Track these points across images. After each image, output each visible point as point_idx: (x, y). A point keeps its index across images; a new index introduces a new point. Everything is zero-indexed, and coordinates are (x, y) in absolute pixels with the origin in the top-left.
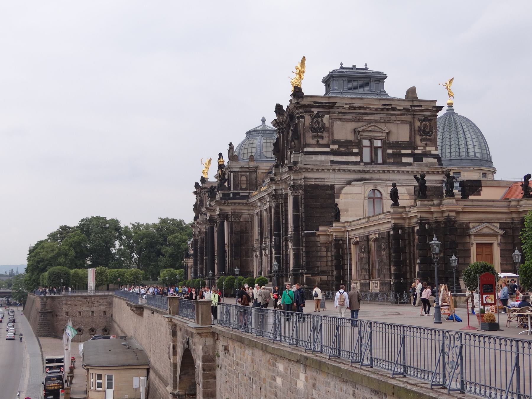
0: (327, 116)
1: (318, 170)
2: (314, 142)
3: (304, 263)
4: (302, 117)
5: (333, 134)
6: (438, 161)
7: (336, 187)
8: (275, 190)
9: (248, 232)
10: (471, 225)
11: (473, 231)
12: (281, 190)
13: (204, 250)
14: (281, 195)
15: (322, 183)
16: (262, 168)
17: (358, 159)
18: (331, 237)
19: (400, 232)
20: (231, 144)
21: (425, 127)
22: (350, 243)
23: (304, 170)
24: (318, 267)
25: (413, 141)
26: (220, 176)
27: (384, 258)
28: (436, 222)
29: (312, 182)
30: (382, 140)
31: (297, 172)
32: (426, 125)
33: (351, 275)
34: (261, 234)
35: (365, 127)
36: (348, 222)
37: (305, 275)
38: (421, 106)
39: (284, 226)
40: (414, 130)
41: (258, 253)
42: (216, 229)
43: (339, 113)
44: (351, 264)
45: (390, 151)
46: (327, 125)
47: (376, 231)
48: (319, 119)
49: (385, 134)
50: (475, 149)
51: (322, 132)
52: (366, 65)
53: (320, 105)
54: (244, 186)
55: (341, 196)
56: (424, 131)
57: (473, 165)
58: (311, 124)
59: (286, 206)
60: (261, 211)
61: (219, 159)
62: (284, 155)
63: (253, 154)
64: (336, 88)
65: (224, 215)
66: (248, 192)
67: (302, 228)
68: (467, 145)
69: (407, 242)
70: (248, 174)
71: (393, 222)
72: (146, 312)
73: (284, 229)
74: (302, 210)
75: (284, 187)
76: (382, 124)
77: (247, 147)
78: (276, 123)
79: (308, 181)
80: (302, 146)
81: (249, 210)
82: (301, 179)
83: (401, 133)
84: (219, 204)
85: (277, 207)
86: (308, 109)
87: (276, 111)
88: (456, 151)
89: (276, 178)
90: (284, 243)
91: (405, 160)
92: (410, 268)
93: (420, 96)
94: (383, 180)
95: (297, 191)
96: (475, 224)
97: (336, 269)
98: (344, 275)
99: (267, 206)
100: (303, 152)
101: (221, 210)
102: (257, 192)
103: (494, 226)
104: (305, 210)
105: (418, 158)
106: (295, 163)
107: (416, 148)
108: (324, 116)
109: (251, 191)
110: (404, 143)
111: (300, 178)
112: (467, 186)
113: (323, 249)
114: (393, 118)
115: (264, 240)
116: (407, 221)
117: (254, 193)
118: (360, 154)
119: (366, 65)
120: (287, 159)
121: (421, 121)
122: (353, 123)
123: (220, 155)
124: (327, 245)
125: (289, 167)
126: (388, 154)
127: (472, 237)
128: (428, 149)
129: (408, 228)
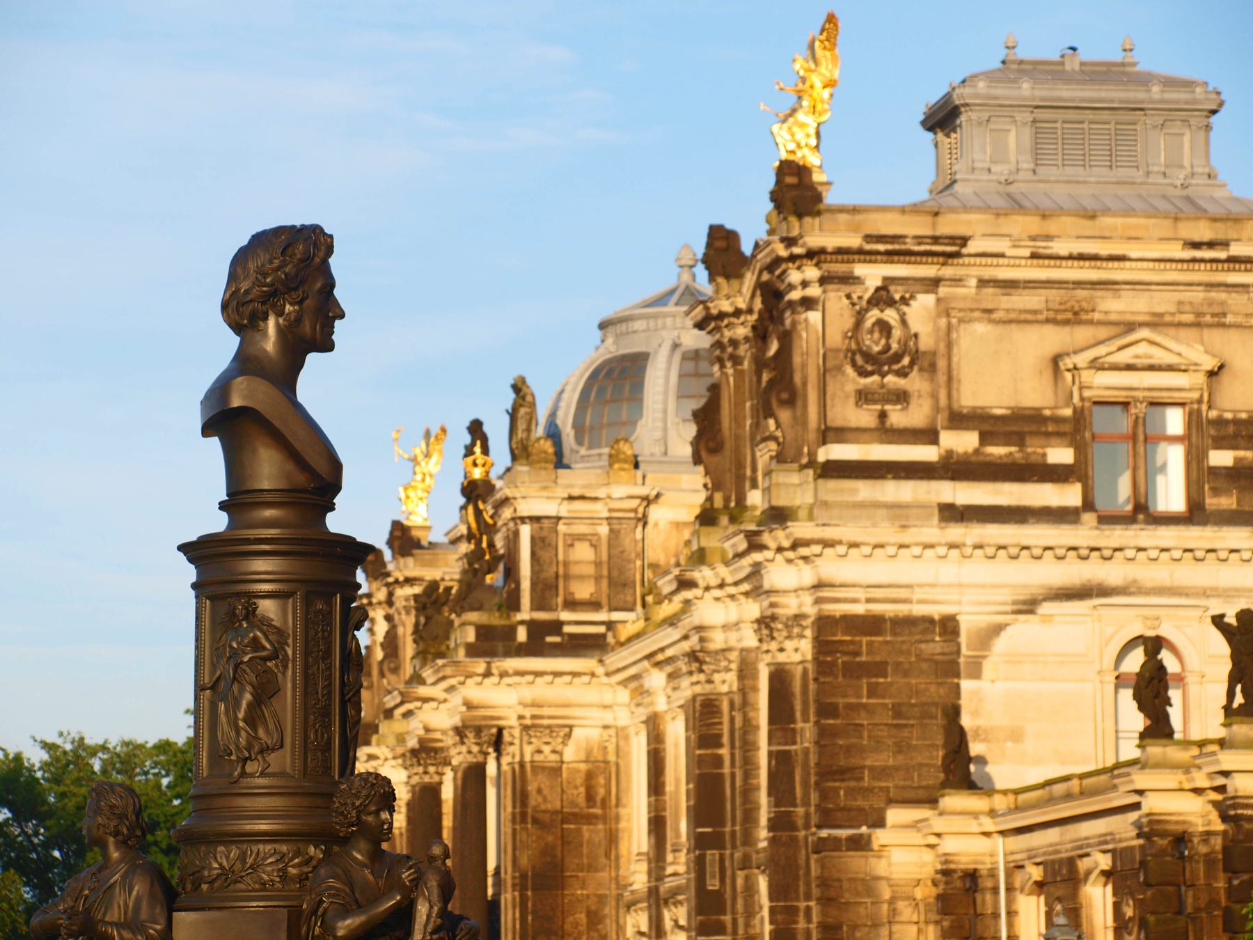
0: (925, 301)
2: (865, 417)
4: (808, 303)
7: (967, 624)
17: (1071, 495)
20: (519, 388)
29: (854, 601)
34: (657, 825)
35: (1101, 350)
45: (1221, 458)
46: (925, 343)
48: (890, 315)
49: (1200, 379)
51: (903, 373)
54: (583, 591)
55: (988, 667)
62: (740, 466)
66: (602, 616)
74: (806, 730)
79: (837, 600)
94: (1187, 595)
95: (789, 645)
100: (812, 463)
108: (912, 297)
109: (616, 616)
117: (630, 621)
122: (1049, 330)
123: (476, 429)
125: (750, 535)
126: (1214, 471)
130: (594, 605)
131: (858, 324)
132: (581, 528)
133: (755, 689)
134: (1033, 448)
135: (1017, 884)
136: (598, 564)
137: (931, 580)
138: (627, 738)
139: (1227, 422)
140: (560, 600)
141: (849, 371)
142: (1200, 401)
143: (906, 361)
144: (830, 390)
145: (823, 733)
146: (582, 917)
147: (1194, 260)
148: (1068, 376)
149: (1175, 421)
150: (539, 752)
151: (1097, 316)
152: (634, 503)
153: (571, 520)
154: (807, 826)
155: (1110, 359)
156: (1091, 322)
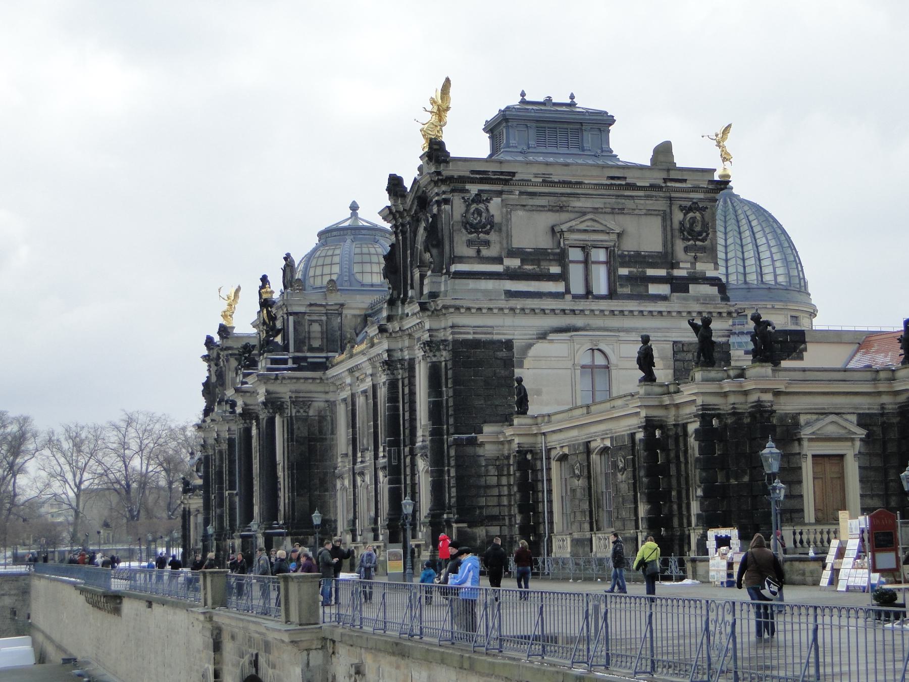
0: (496, 201)
1: (480, 309)
2: (471, 252)
3: (453, 500)
4: (446, 201)
5: (509, 236)
6: (720, 292)
7: (516, 344)
8: (388, 351)
9: (326, 439)
10: (803, 419)
11: (806, 433)
12: (401, 350)
13: (226, 477)
14: (401, 361)
15: (489, 337)
16: (354, 305)
17: (560, 287)
18: (506, 446)
19: (658, 433)
20: (287, 258)
21: (694, 222)
22: (548, 458)
23: (452, 310)
24: (481, 508)
25: (670, 250)
26: (264, 323)
27: (624, 487)
28: (734, 414)
29: (468, 333)
30: (607, 248)
31: (436, 313)
32: (693, 220)
33: (551, 523)
35: (573, 223)
36: (543, 416)
37: (454, 525)
38: (685, 181)
39: (407, 425)
40: (672, 230)
41: (346, 482)
42: (254, 431)
43: (521, 193)
44: (550, 502)
45: (623, 271)
46: (497, 219)
47: (605, 433)
48: (482, 206)
49: (614, 237)
50: (774, 269)
51: (487, 233)
52: (572, 97)
53: (482, 177)
54: (316, 344)
55: (527, 363)
56: (691, 231)
57: (772, 299)
58: (465, 215)
59: (412, 384)
60: (353, 396)
61: (262, 288)
63: (334, 277)
64: (512, 142)
65: (274, 404)
66: (324, 355)
67: (448, 428)
68: (760, 260)
69: (672, 455)
70: (324, 318)
71: (643, 413)
72: (128, 606)
73: (407, 431)
74: (447, 392)
75: (407, 343)
76: (607, 217)
77: (320, 262)
78: (389, 214)
80: (446, 260)
81: (327, 393)
82: (445, 329)
83: (646, 236)
84: (263, 379)
85: (393, 386)
86: (460, 186)
87: (389, 190)
88: (737, 272)
89: (390, 326)
90: (408, 460)
91: (653, 289)
92: (680, 507)
93: (682, 159)
94: (611, 331)
95: (437, 353)
96: (809, 416)
97: (520, 512)
98: (537, 524)
99: (368, 384)
100: (448, 273)
101: (268, 392)
102: (343, 356)
103: (847, 420)
104: (455, 391)
105: (680, 286)
106: (434, 295)
107: (674, 265)
108: (491, 199)
109: (330, 354)
110: (651, 255)
111: (445, 327)
112: (778, 342)
113: (492, 471)
114: (629, 204)
115: (359, 455)
116: (673, 412)
117: (338, 357)
118: (563, 277)
119: (572, 97)
120: (412, 288)
121: (686, 210)
122: (550, 214)
123: (264, 279)
124: (500, 464)
125: (421, 304)
126: (621, 277)
127: (805, 443)
128: (700, 267)
129: (674, 425)
130: (320, 349)
131: (467, 211)
132: (315, 318)
133: (414, 377)
134: (544, 264)
135: (552, 457)
136: (322, 333)
137: (501, 324)
138: (335, 405)
139: (625, 256)
140: (306, 348)
141: (464, 231)
142: (614, 246)
143: (489, 227)
144: (456, 239)
145: (456, 394)
146: (317, 481)
147: (612, 185)
148: (558, 235)
149: (601, 255)
150: (299, 412)
151: (570, 209)
152: (337, 307)
153: (310, 314)
154: (448, 434)
155: (576, 227)
156: (567, 211)
